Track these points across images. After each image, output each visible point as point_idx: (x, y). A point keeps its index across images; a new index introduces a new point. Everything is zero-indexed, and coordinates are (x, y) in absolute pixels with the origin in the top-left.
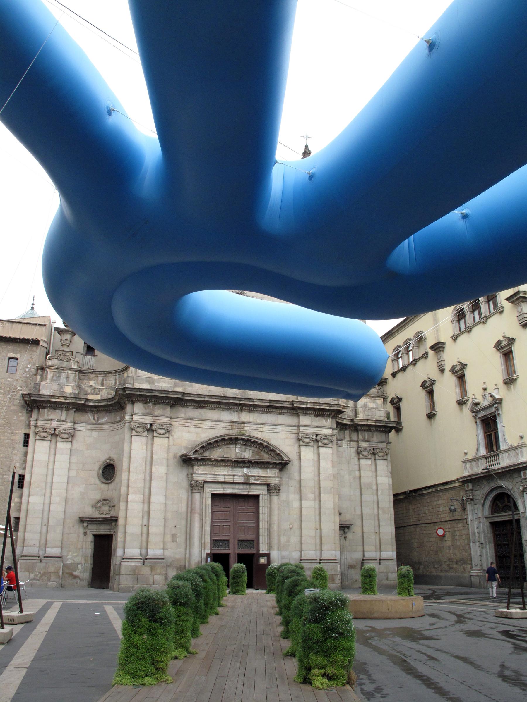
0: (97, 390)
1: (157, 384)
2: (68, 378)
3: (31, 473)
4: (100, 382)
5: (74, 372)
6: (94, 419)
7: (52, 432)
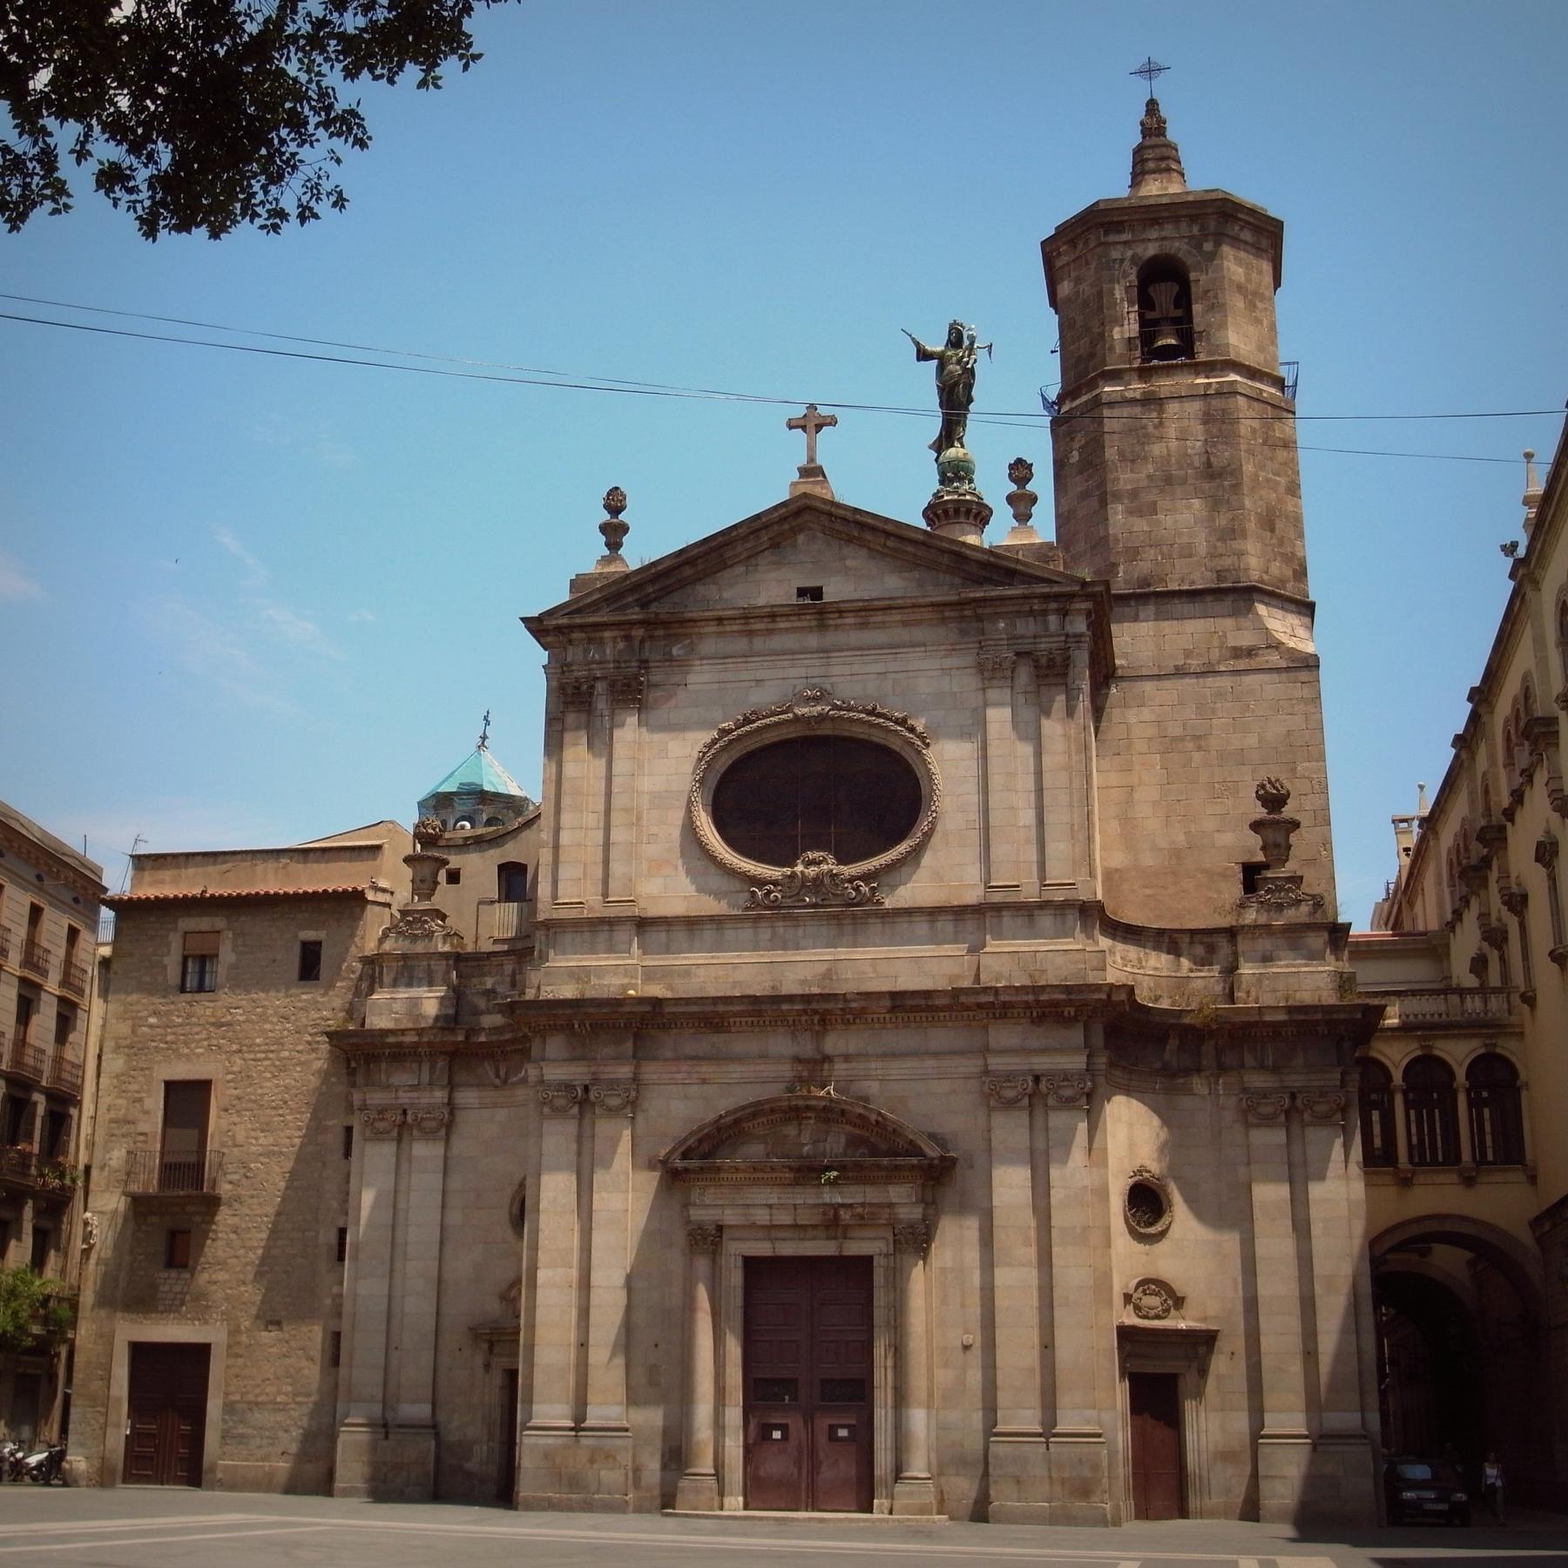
1: (597, 982)
4: (508, 979)
5: (444, 962)
6: (498, 1076)
7: (399, 1119)
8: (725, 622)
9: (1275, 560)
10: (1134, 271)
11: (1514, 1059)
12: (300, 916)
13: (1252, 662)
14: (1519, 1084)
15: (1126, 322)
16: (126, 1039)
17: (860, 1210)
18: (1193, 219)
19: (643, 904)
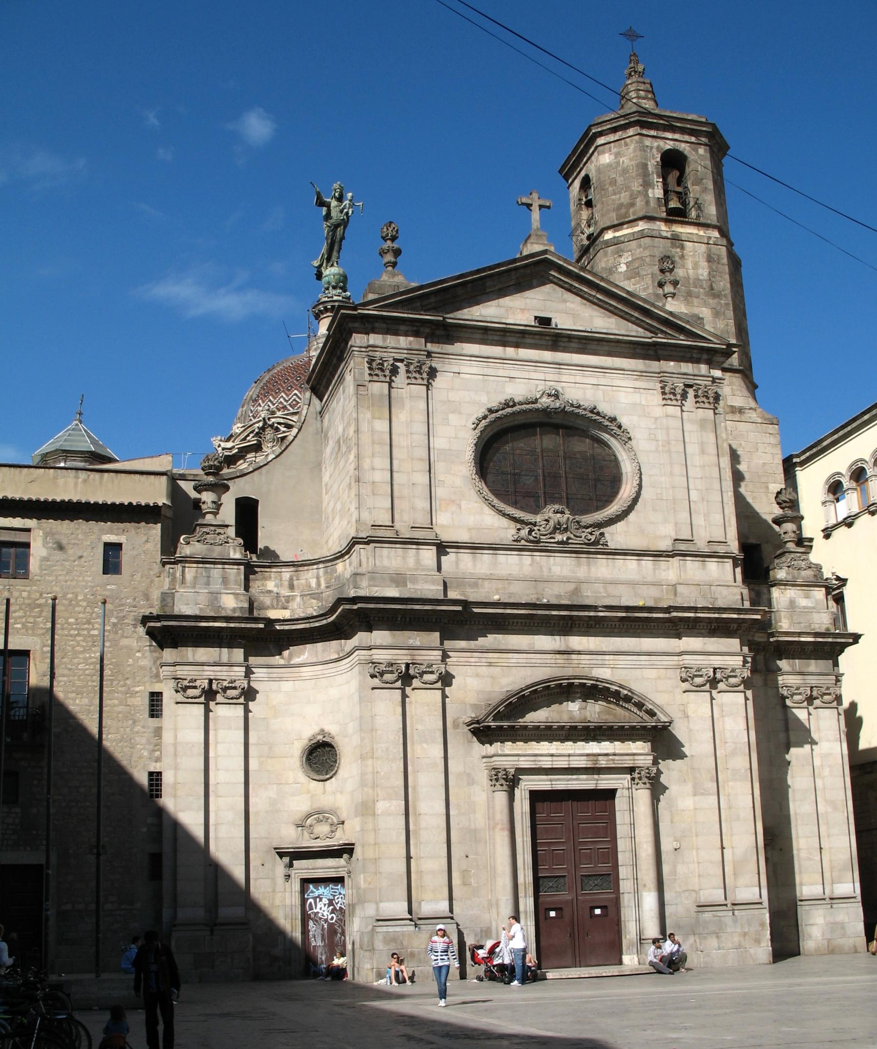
0: (283, 599)
1: (412, 587)
3: (176, 768)
4: (286, 583)
8: (489, 332)
10: (659, 156)
15: (656, 187)
19: (437, 529)
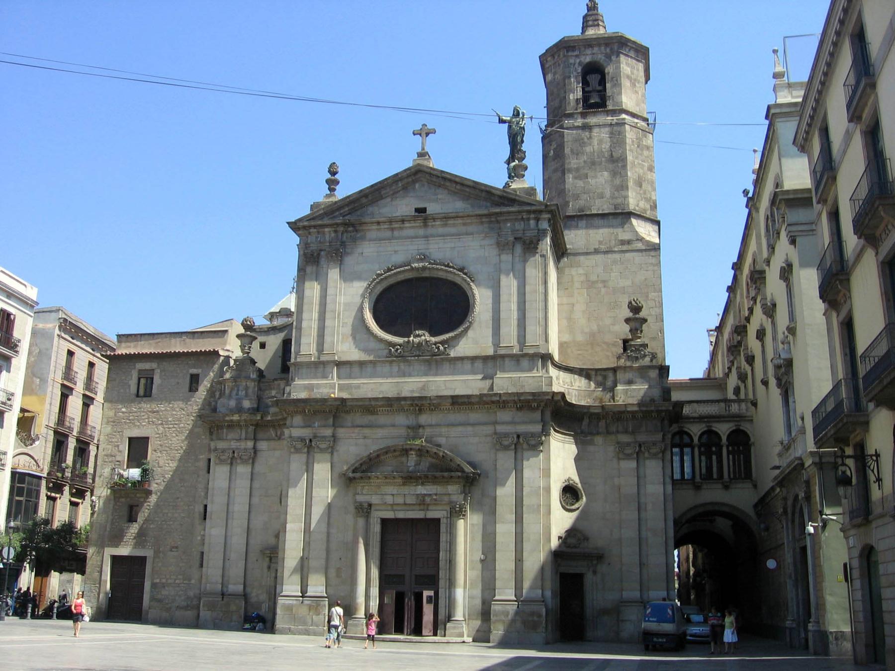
2: (247, 388)
9: (642, 200)
11: (748, 432)
12: (190, 362)
13: (629, 247)
14: (750, 443)
16: (111, 418)
17: (435, 497)
18: (607, 45)
